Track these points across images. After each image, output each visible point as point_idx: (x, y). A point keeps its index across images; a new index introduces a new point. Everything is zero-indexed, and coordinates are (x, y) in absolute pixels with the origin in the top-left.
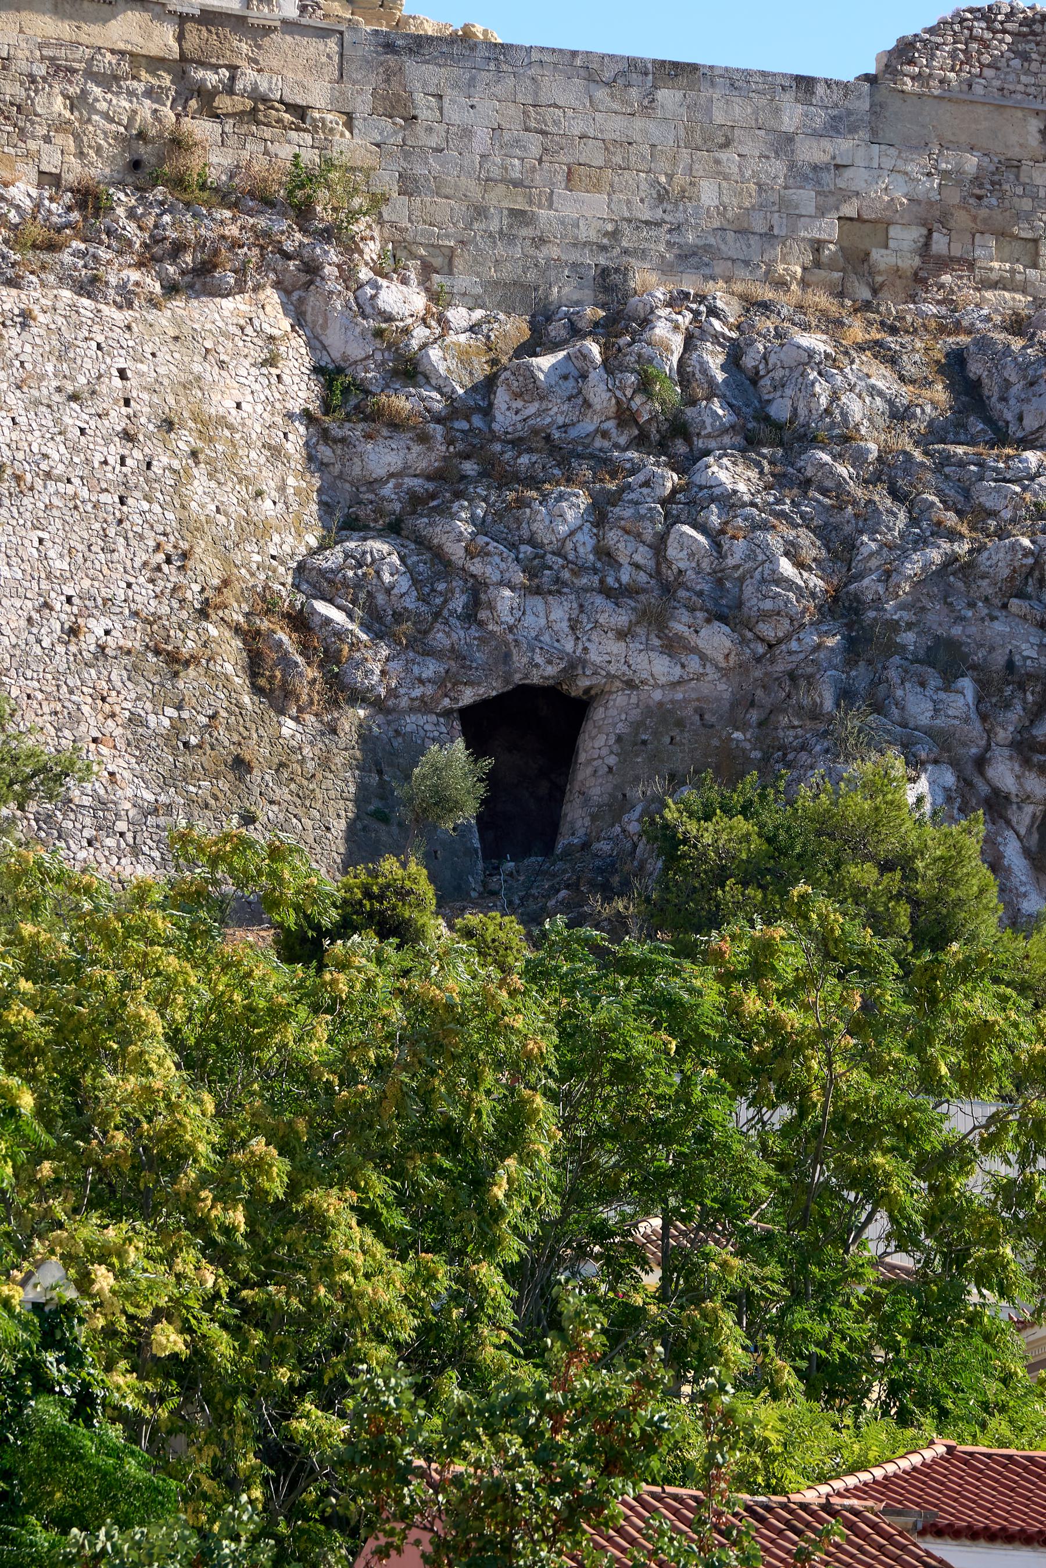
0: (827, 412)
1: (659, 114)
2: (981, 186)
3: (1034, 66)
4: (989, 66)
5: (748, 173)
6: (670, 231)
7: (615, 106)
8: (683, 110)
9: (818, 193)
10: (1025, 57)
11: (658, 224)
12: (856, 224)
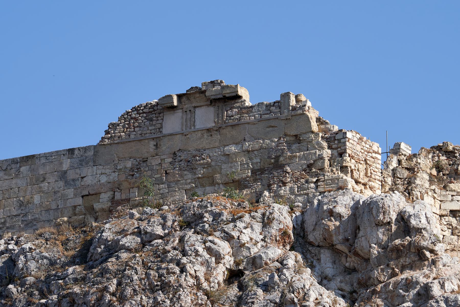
0: (22, 269)
1: (21, 176)
2: (133, 171)
3: (154, 123)
4: (137, 127)
5: (50, 189)
6: (23, 217)
7: (6, 177)
8: (29, 172)
9: (75, 189)
10: (151, 120)
11: (19, 215)
12: (90, 197)
